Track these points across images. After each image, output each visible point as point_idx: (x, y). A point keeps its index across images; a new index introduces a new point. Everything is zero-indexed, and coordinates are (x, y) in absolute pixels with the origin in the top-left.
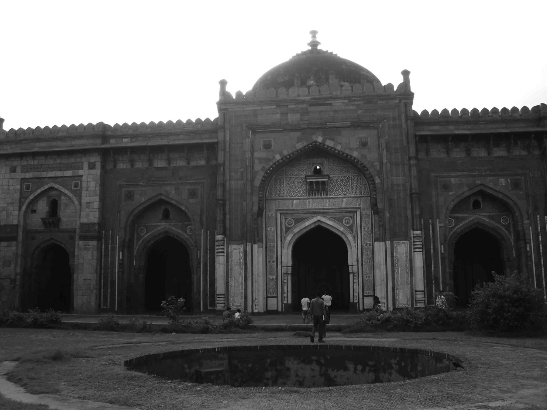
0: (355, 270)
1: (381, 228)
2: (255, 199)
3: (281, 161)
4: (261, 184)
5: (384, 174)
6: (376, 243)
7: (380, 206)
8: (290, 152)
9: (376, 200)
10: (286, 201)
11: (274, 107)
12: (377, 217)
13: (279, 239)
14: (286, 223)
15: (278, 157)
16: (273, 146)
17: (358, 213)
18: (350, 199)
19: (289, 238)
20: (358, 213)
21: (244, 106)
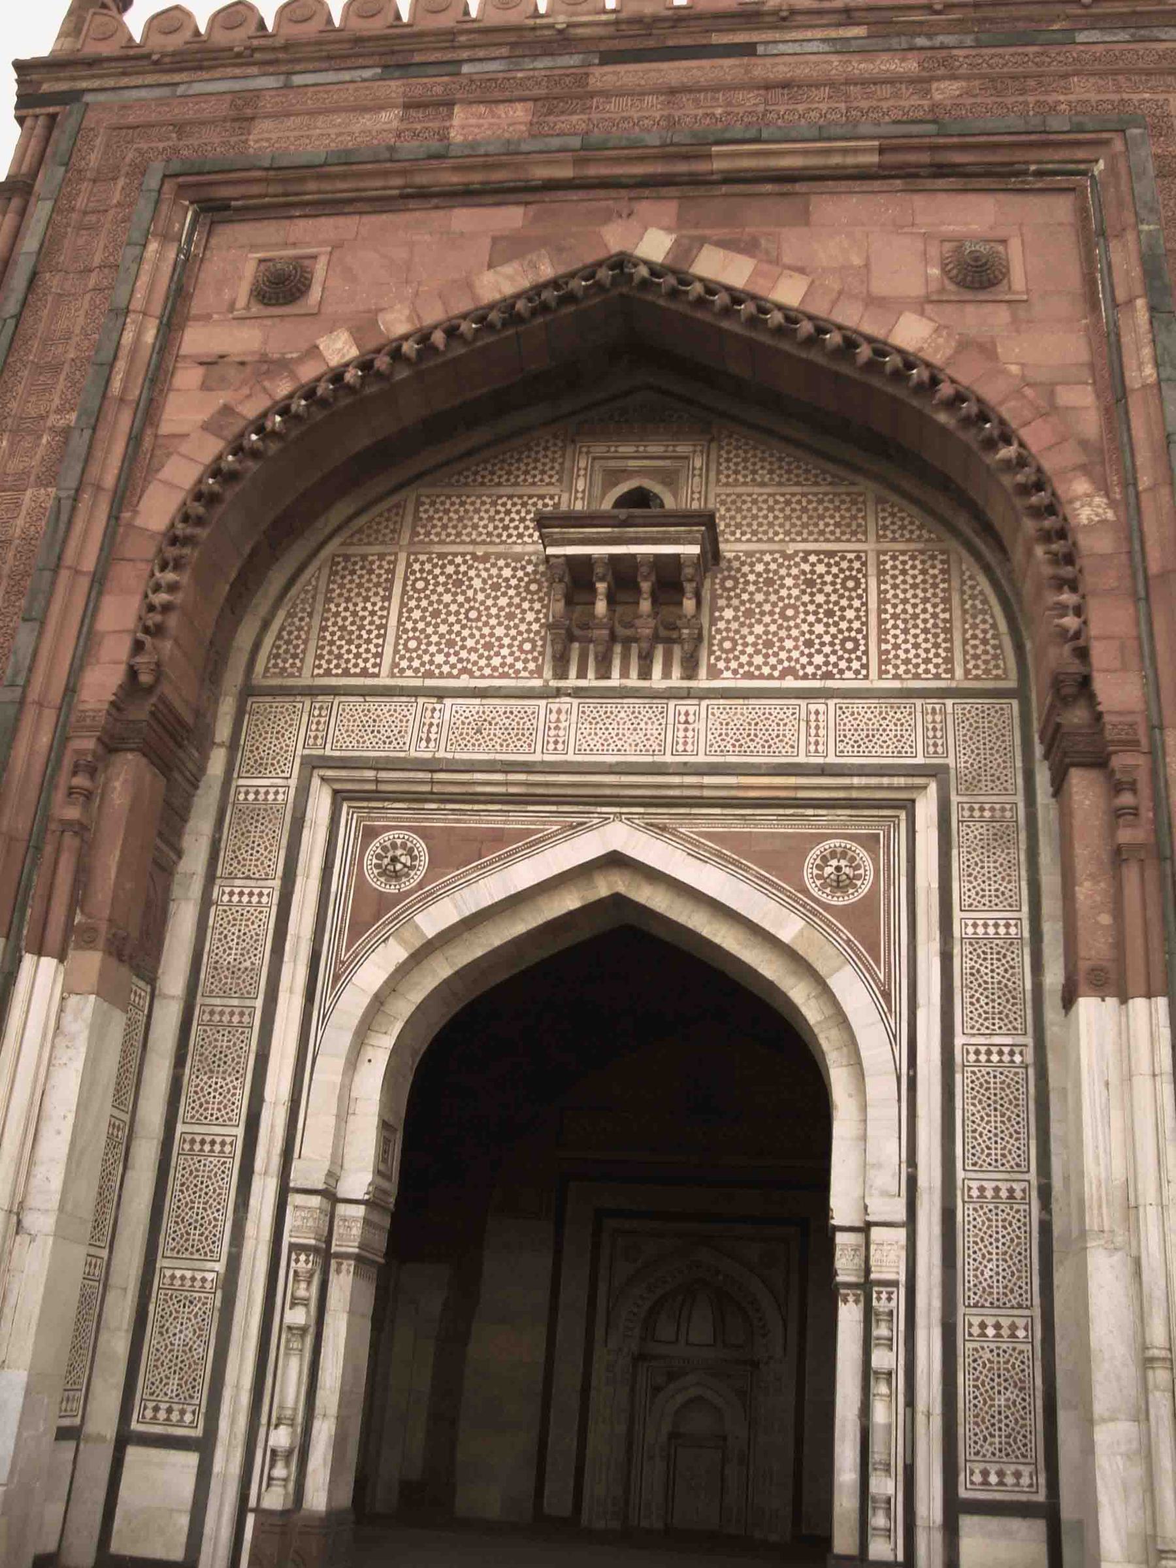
0: (888, 1260)
1: (1131, 875)
2: (119, 614)
3: (351, 376)
4: (186, 518)
5: (1143, 457)
6: (1087, 1006)
7: (1117, 691)
8: (433, 314)
9: (1083, 654)
10: (381, 708)
11: (367, 73)
12: (1084, 787)
13: (294, 975)
14: (370, 860)
15: (339, 349)
16: (315, 293)
17: (926, 809)
18: (859, 705)
19: (372, 973)
20: (926, 809)
21: (177, 78)
